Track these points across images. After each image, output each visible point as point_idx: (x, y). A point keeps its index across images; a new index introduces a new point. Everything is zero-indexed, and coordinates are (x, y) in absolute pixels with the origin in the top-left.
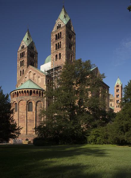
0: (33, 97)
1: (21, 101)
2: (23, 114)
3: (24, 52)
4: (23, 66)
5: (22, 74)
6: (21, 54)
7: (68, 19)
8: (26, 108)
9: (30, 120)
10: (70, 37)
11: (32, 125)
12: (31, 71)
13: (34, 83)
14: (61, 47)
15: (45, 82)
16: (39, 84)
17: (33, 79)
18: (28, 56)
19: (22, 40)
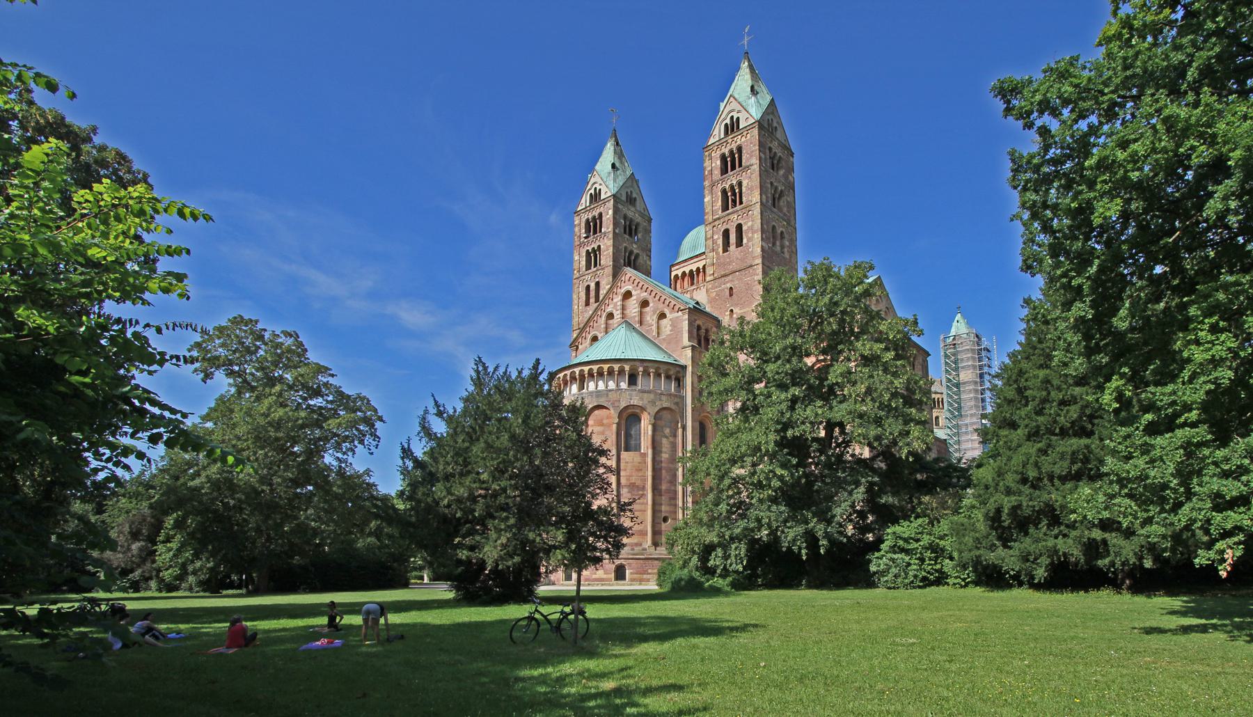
0: (643, 392)
3: (600, 215)
4: (595, 266)
5: (592, 300)
6: (588, 220)
7: (766, 99)
12: (629, 287)
15: (686, 335)
16: (664, 339)
17: (641, 323)
18: (617, 231)
19: (591, 169)
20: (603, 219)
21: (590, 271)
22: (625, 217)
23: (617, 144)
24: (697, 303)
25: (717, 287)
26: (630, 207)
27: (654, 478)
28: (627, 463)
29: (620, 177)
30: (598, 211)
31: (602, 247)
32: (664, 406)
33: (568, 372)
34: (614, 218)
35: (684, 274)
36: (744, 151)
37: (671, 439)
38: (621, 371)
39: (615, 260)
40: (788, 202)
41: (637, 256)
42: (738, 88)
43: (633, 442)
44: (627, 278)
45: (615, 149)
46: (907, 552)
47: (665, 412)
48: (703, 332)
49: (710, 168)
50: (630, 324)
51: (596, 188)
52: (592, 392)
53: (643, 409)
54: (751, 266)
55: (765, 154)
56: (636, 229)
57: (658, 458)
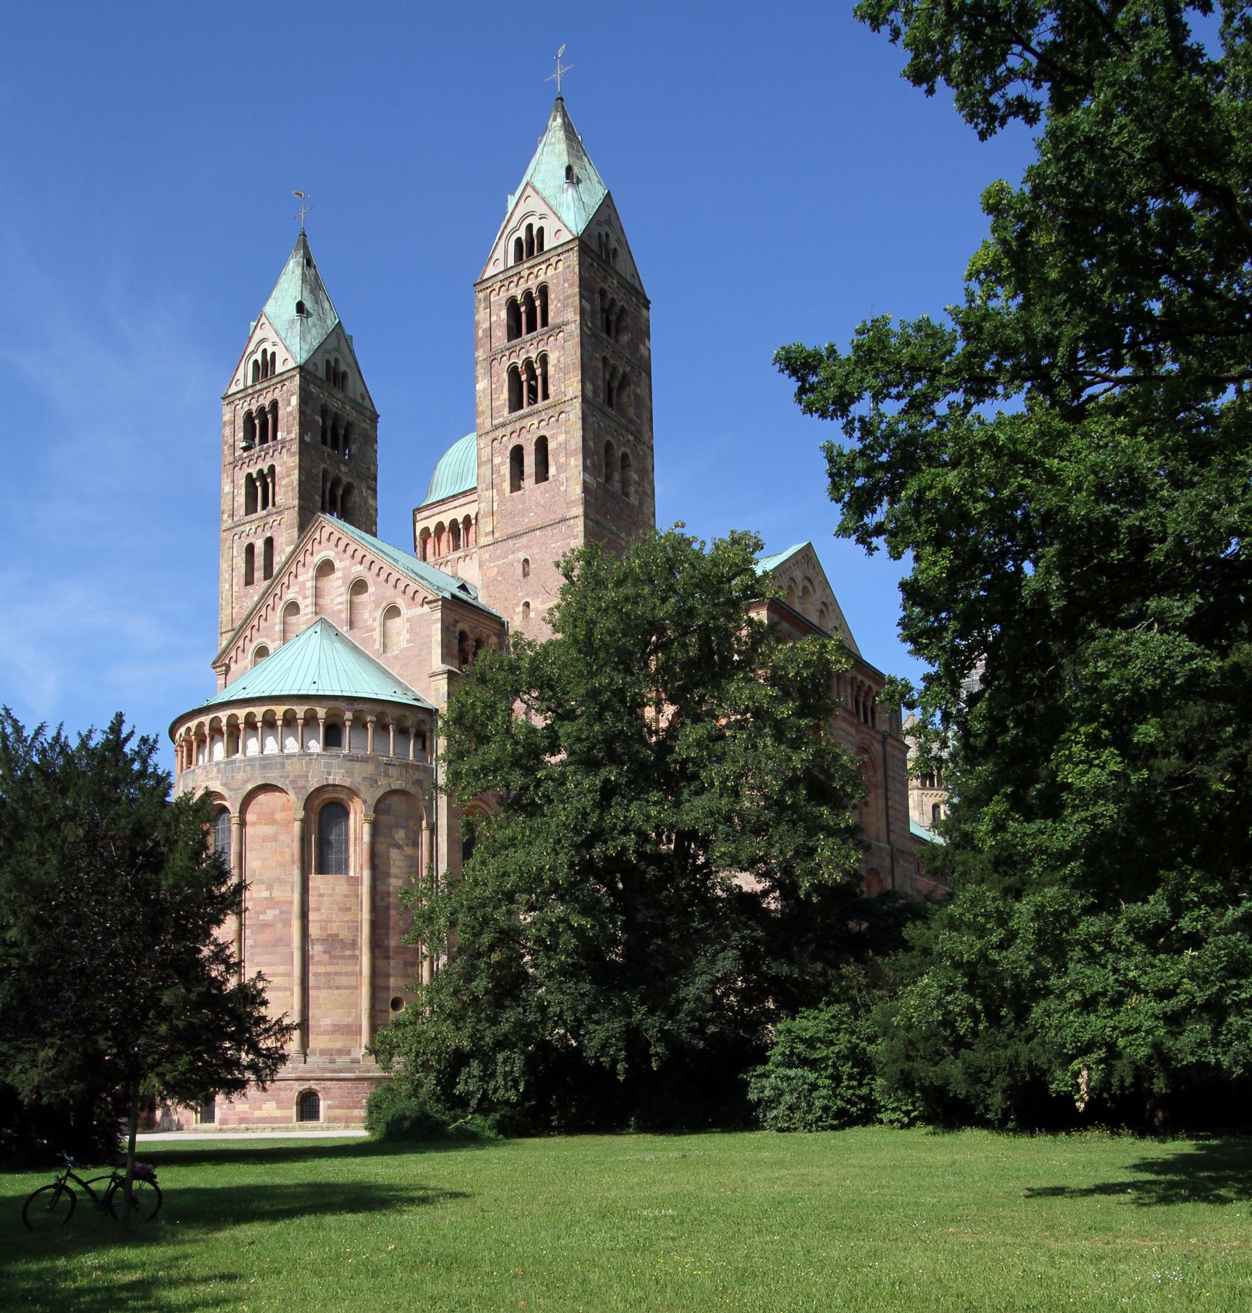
0: (352, 759)
1: (262, 798)
2: (277, 894)
3: (274, 404)
4: (265, 506)
5: (259, 574)
6: (249, 413)
7: (594, 193)
8: (296, 846)
9: (332, 941)
10: (608, 323)
11: (343, 981)
13: (355, 649)
14: (551, 389)
15: (437, 652)
16: (396, 657)
17: (351, 624)
18: (307, 439)
19: (256, 312)
20: (281, 413)
21: (254, 516)
22: (324, 412)
23: (309, 263)
24: (463, 587)
25: (499, 558)
26: (335, 391)
27: (374, 925)
28: (321, 895)
29: (314, 331)
30: (270, 397)
31: (278, 469)
32: (394, 787)
33: (206, 719)
34: (302, 412)
35: (440, 527)
36: (552, 296)
37: (408, 850)
38: (310, 720)
39: (304, 494)
40: (637, 396)
41: (349, 489)
42: (543, 168)
43: (333, 857)
44: (325, 535)
45: (304, 274)
46: (812, 1064)
47: (396, 798)
48: (471, 643)
49: (486, 325)
50: (331, 626)
51: (265, 351)
52: (253, 759)
53: (352, 792)
54: (564, 520)
55: (591, 301)
56: (346, 436)
57: (381, 888)
